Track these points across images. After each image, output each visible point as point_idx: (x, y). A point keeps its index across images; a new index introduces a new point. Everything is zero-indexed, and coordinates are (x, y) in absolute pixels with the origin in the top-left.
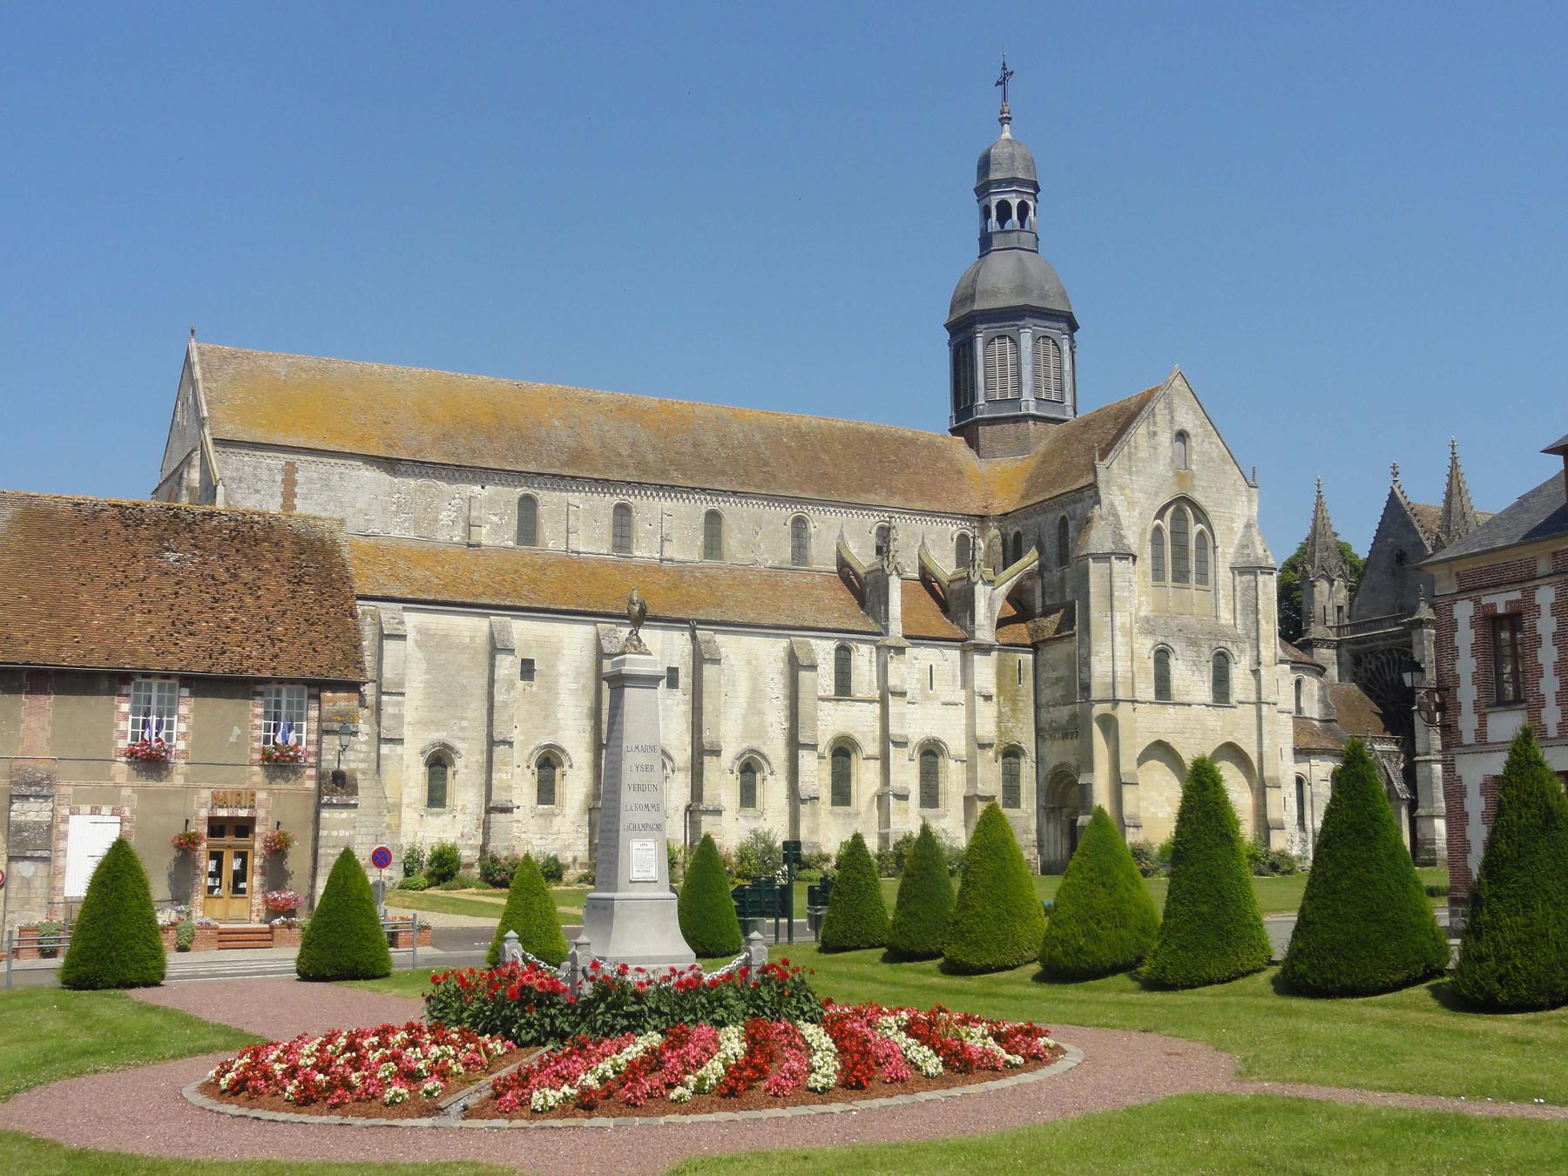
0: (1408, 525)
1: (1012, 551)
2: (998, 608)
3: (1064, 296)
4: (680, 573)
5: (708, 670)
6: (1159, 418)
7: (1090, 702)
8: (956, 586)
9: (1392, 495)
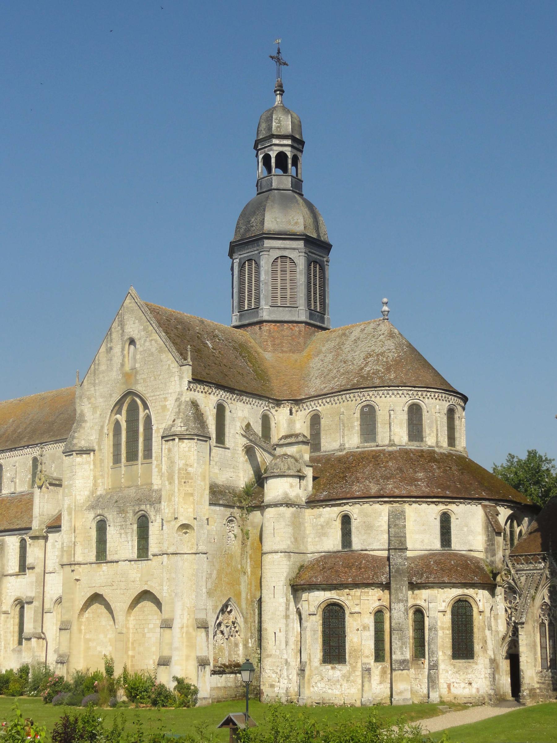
6: (115, 336)
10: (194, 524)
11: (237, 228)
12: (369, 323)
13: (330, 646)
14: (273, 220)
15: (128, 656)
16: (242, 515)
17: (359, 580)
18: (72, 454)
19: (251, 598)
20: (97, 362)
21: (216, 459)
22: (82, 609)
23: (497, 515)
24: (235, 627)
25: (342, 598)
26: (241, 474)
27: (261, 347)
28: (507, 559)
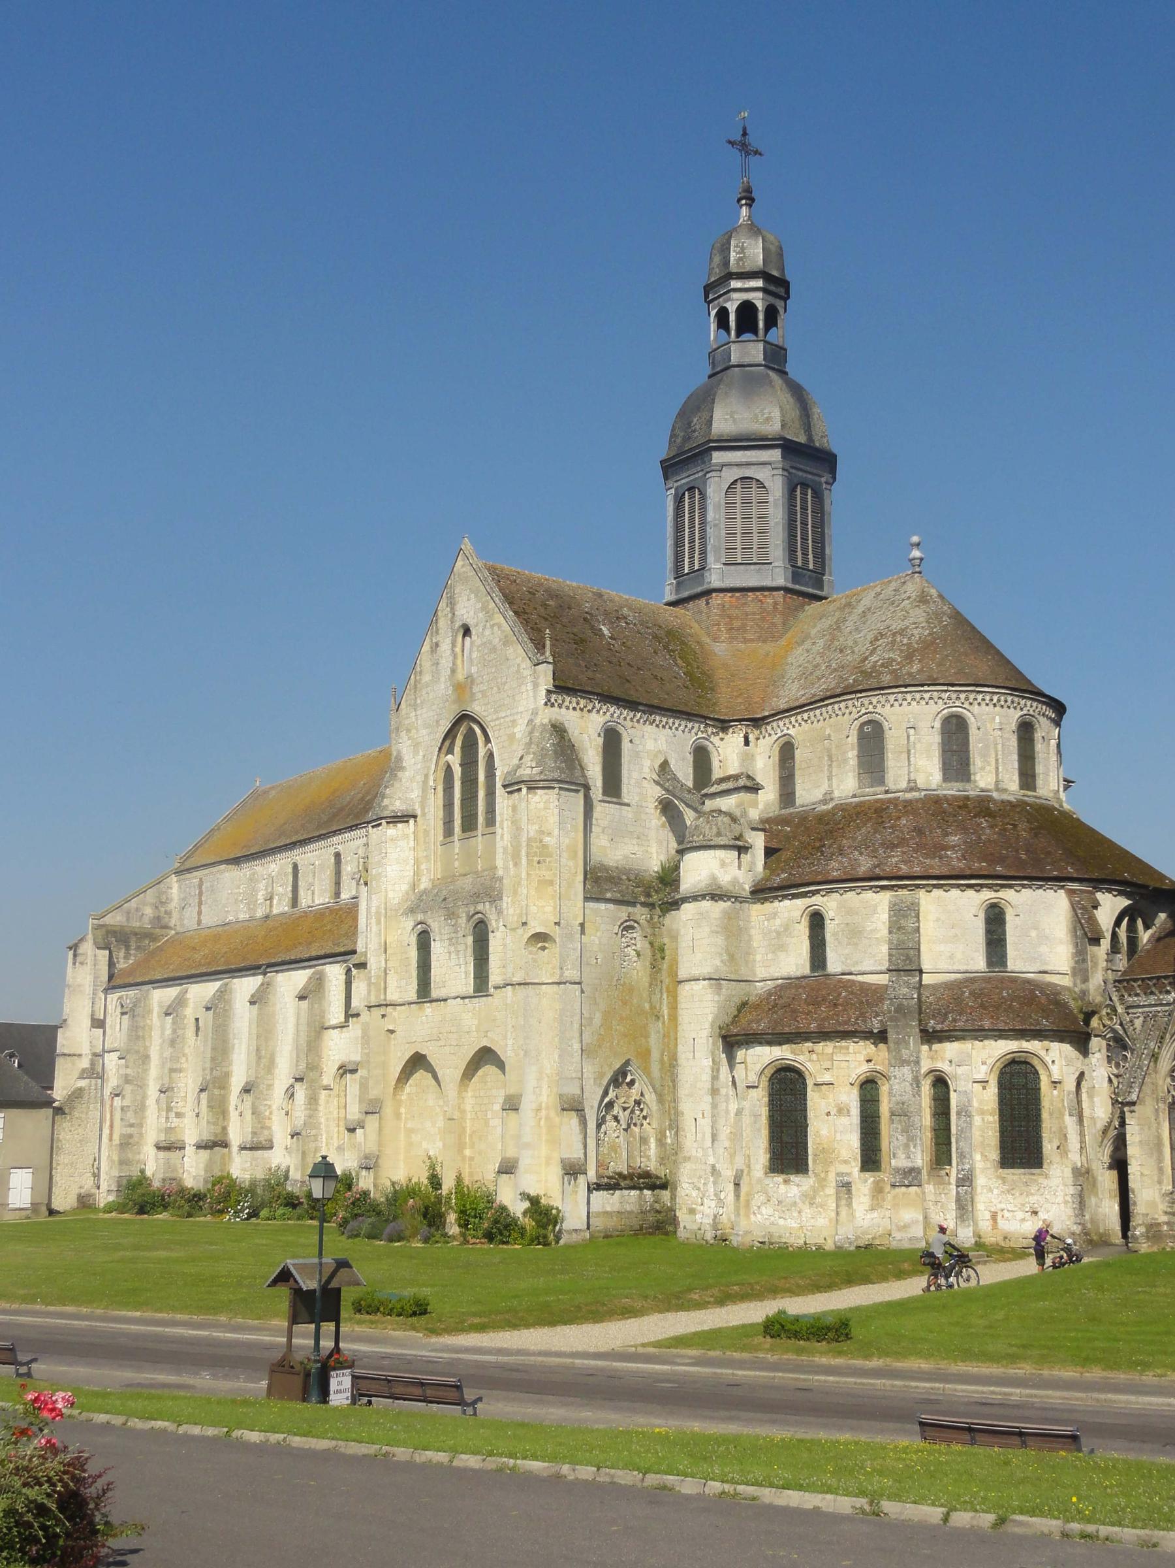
10: (556, 932)
11: (671, 437)
12: (890, 582)
13: (781, 1142)
14: (727, 418)
15: (464, 1158)
16: (651, 919)
17: (828, 1026)
18: (380, 825)
19: (670, 1059)
20: (418, 669)
21: (604, 823)
22: (399, 1080)
23: (1095, 907)
24: (642, 1110)
25: (801, 1058)
26: (653, 849)
27: (708, 634)
28: (1110, 986)
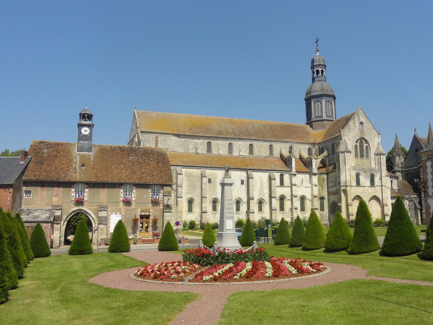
0: (419, 143)
1: (321, 151)
2: (318, 165)
3: (332, 91)
4: (244, 158)
5: (250, 180)
6: (356, 119)
7: (340, 187)
8: (308, 160)
9: (415, 135)
